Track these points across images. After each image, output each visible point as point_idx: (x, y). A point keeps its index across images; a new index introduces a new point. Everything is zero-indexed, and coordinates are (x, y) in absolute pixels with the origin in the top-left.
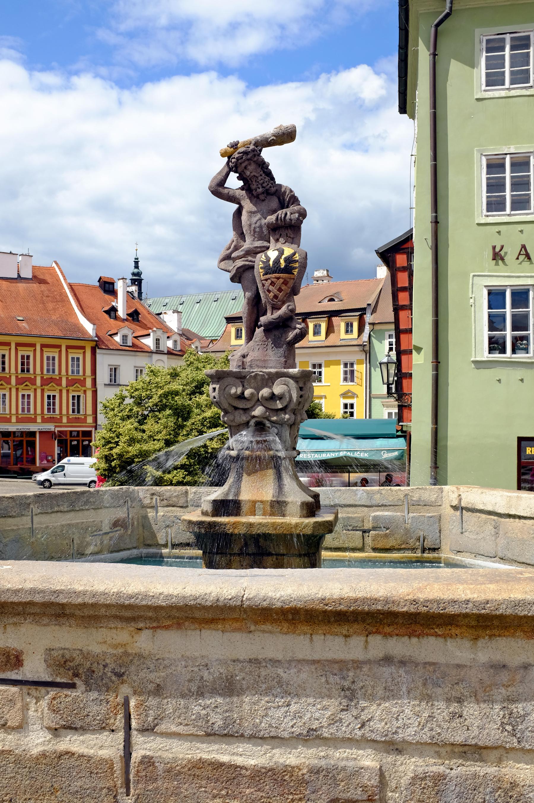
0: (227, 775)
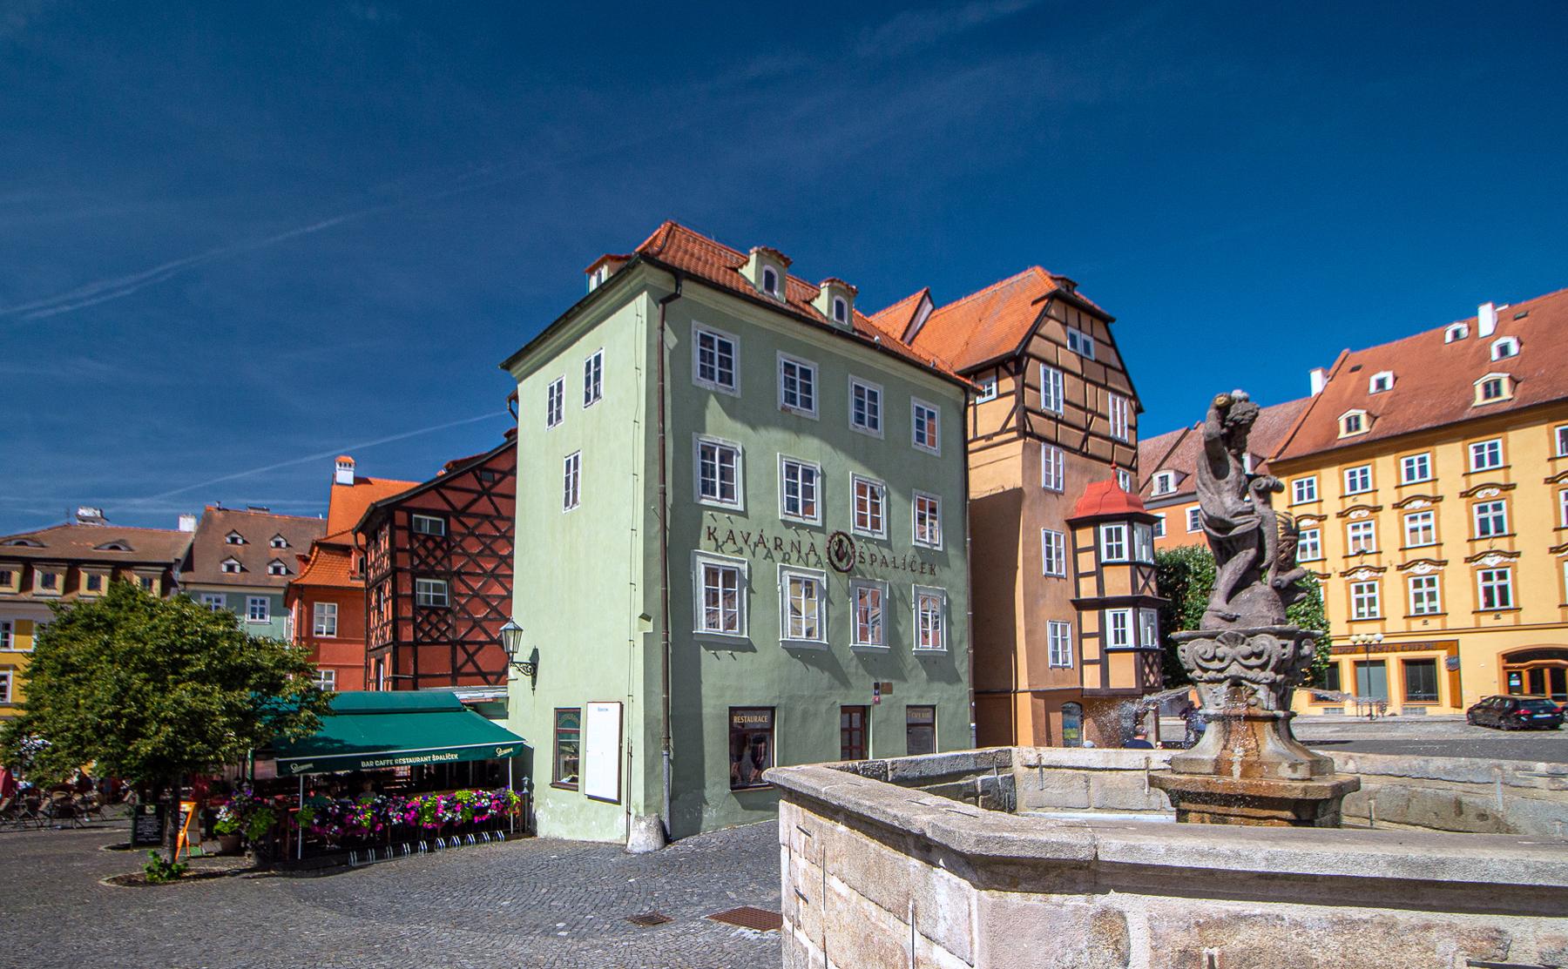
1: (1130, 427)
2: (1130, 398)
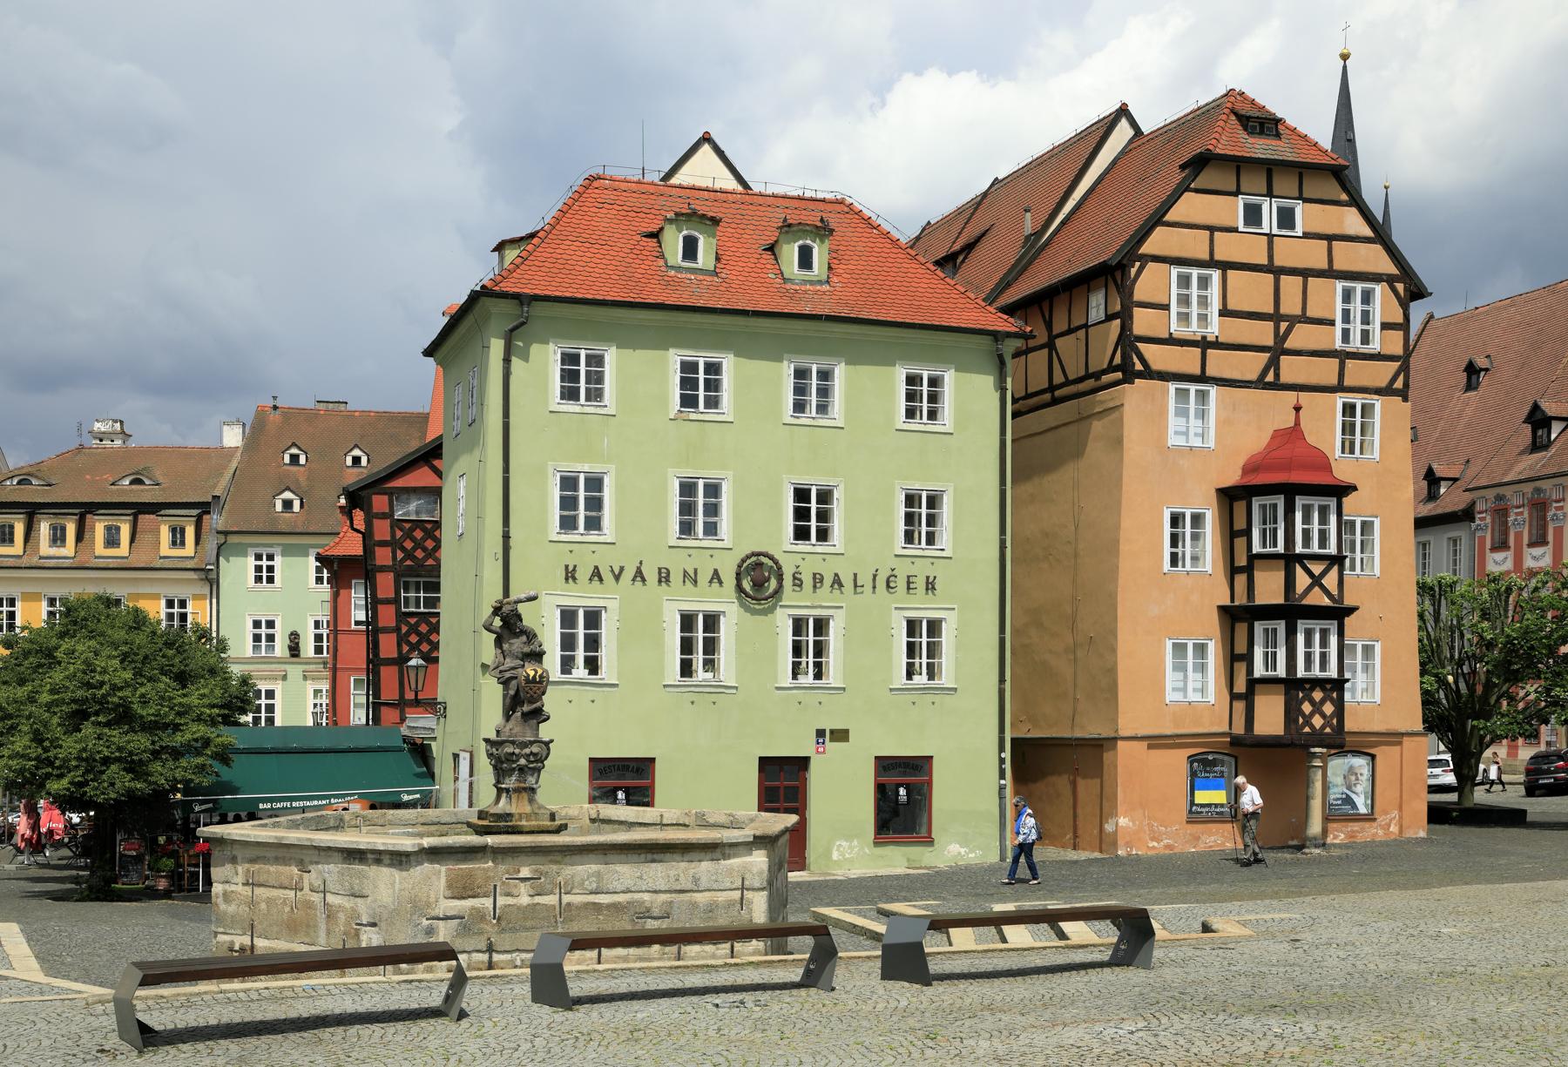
0: (597, 907)
1: (1385, 326)
2: (1390, 280)
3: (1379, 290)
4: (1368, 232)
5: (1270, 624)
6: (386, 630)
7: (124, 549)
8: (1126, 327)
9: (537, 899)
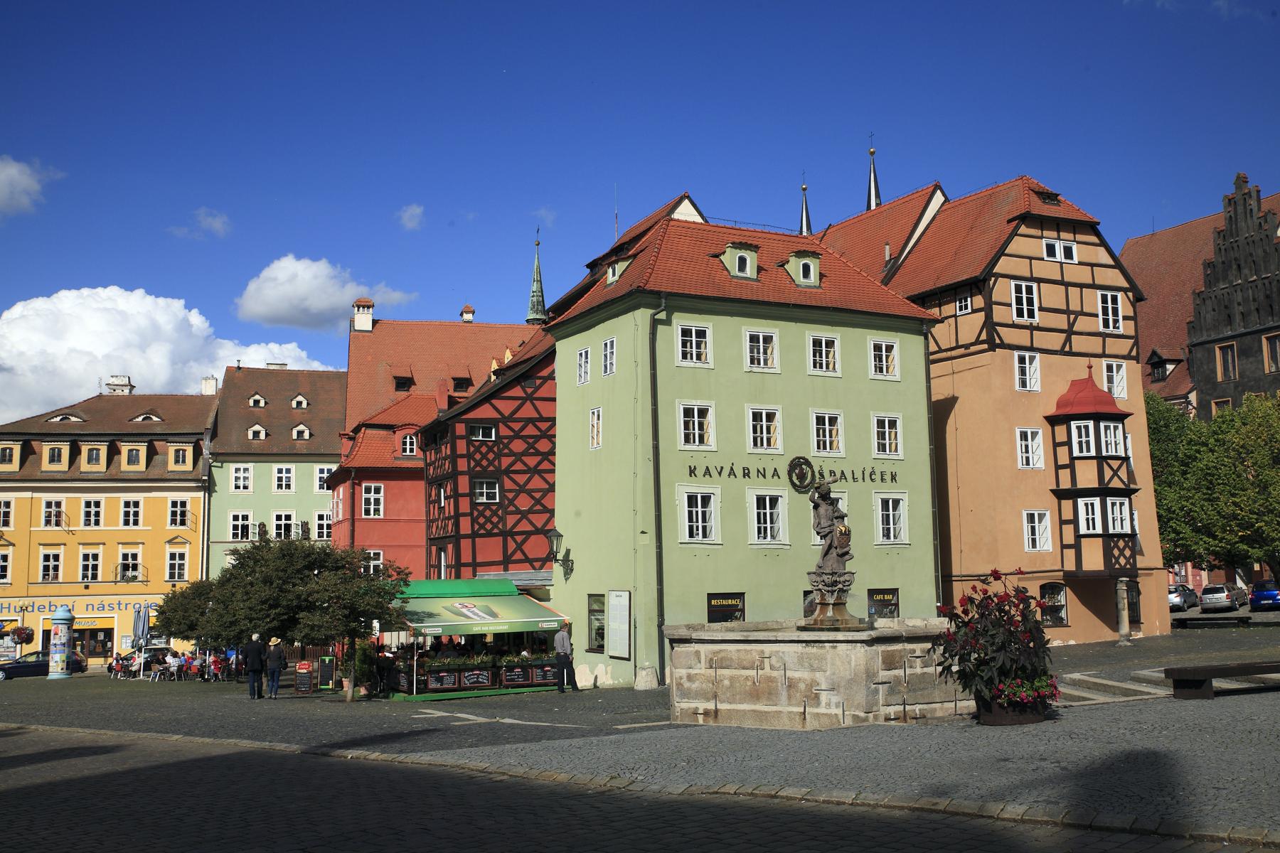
1: (1125, 318)
3: (1120, 295)
4: (1112, 262)
5: (1089, 500)
6: (464, 515)
7: (142, 466)
8: (989, 316)
9: (926, 670)
